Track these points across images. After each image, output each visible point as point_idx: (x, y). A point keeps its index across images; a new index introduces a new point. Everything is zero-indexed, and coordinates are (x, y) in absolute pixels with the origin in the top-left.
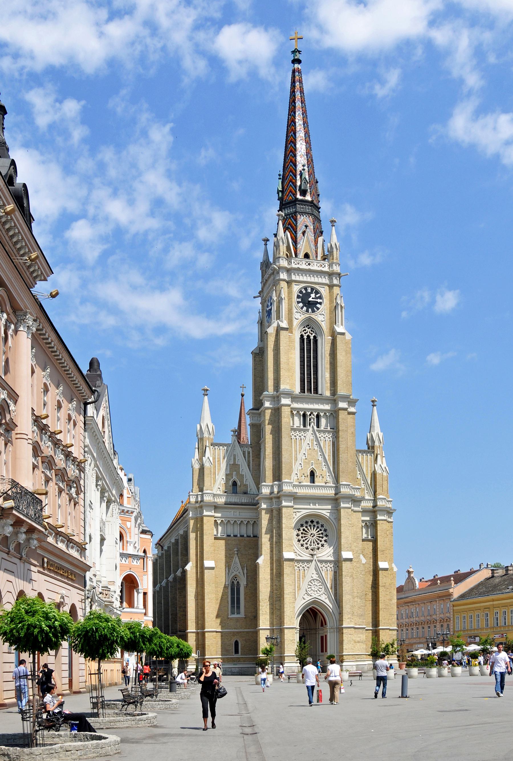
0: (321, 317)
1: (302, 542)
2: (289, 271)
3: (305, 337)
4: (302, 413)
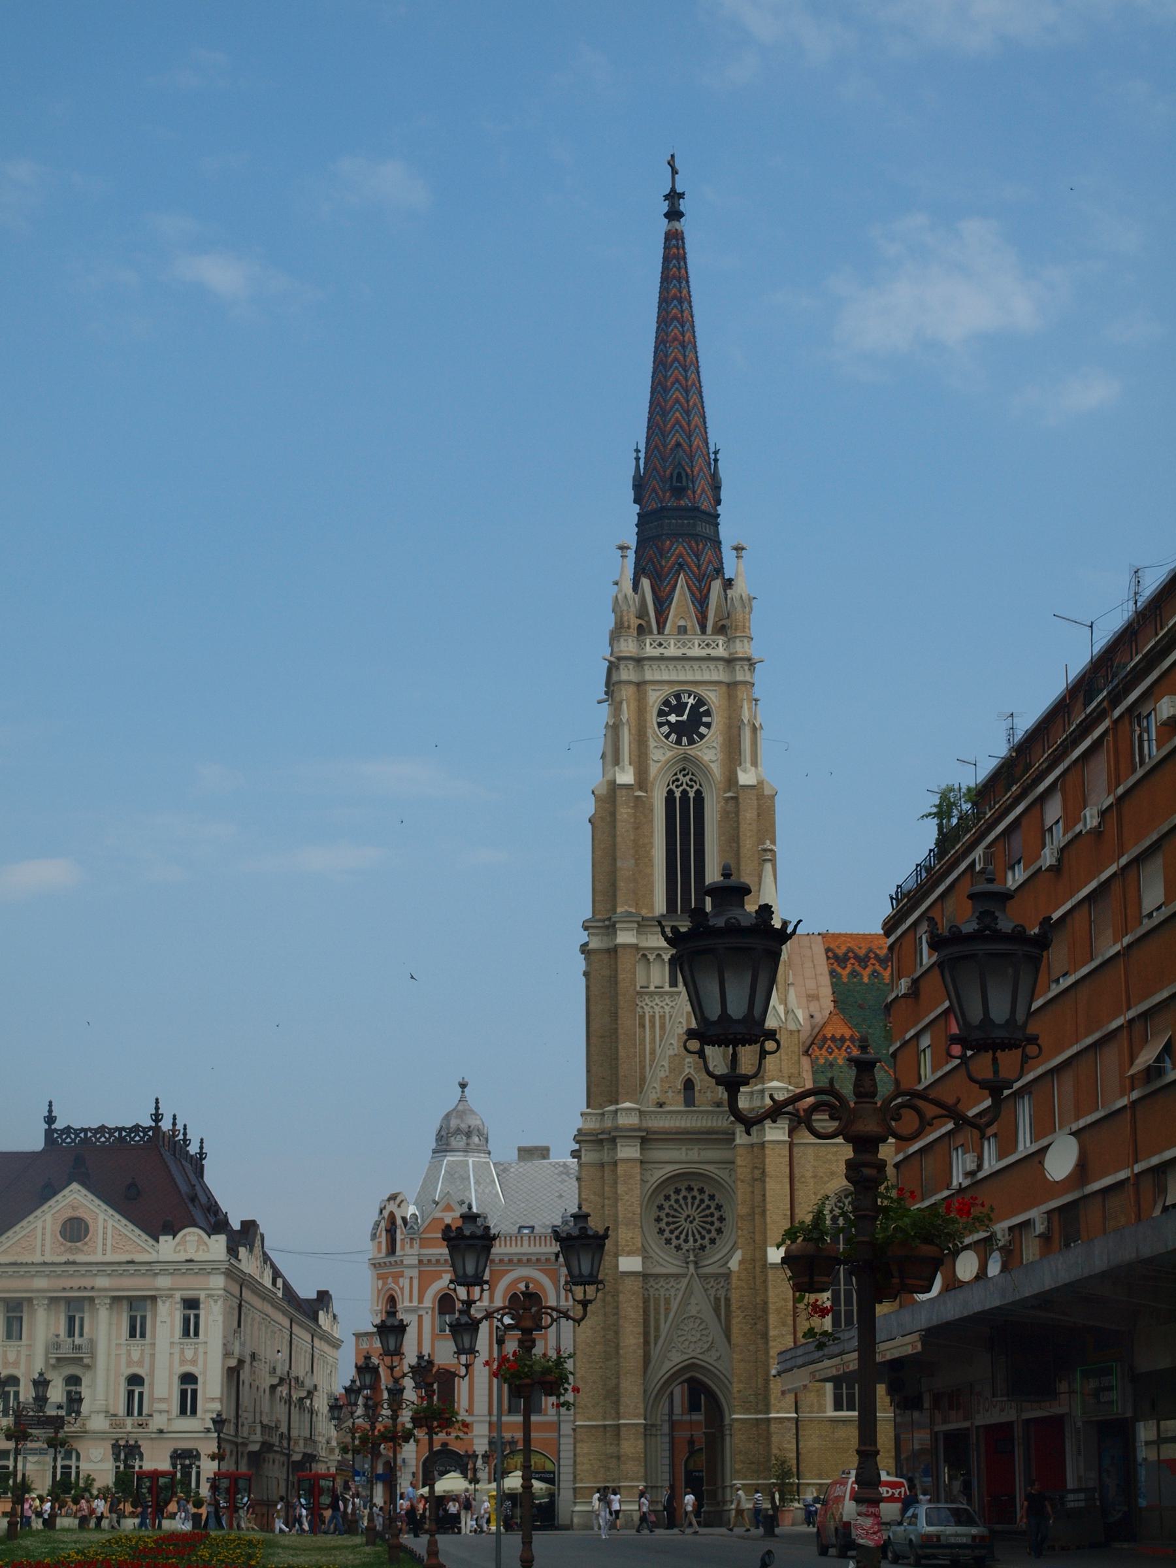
0: (709, 751)
1: (667, 1234)
2: (639, 661)
3: (678, 795)
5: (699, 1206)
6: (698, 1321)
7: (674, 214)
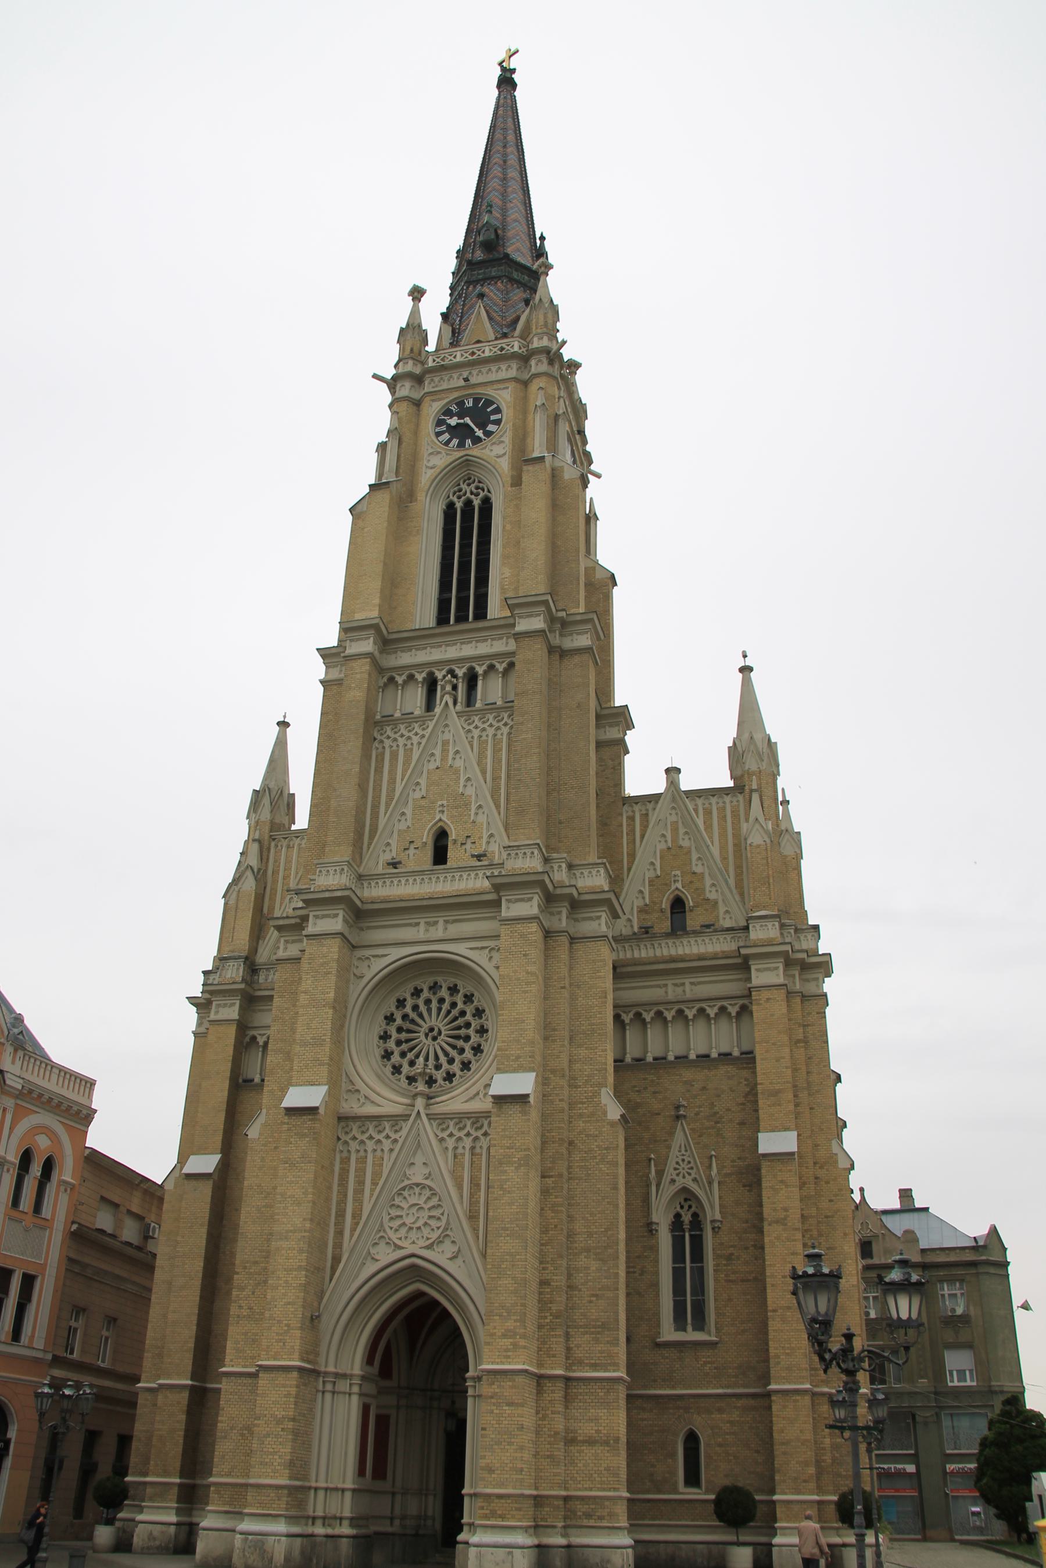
1: (396, 1058)
3: (459, 505)
4: (420, 677)
5: (449, 1012)
6: (428, 1193)
7: (507, 82)
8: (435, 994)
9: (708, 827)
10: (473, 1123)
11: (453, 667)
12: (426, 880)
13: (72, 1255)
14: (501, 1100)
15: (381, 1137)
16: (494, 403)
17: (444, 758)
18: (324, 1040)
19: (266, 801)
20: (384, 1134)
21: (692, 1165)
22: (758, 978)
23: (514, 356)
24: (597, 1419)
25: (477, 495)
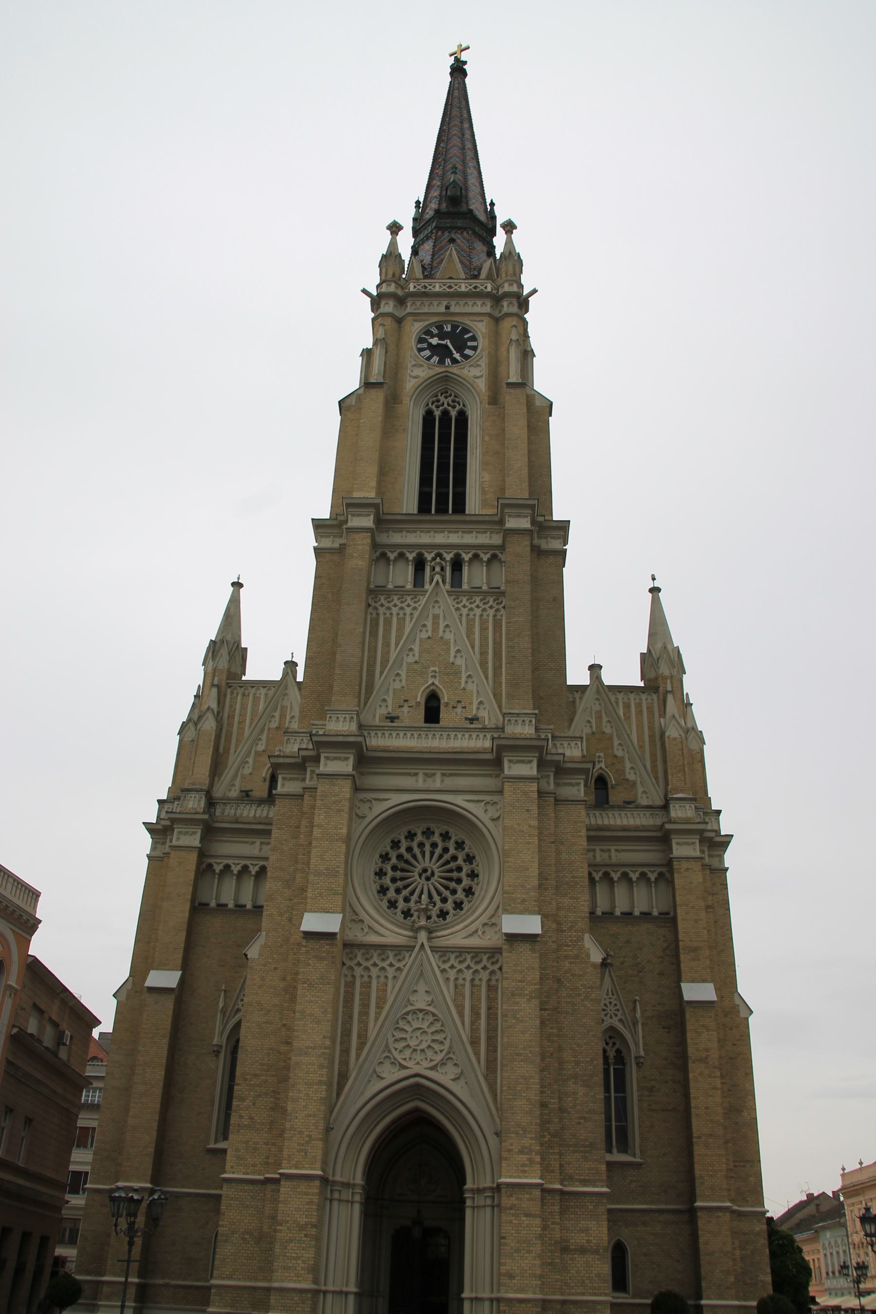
1: (391, 894)
3: (437, 413)
4: (411, 556)
5: (441, 856)
6: (431, 1019)
7: (458, 70)
8: (428, 838)
9: (628, 718)
10: (473, 958)
11: (442, 551)
12: (423, 736)
13: (11, 1059)
14: (513, 938)
15: (385, 965)
16: (469, 332)
17: (435, 629)
18: (338, 872)
19: (224, 651)
20: (388, 962)
21: (618, 1007)
22: (678, 850)
23: (488, 295)
24: (586, 1230)
25: (454, 407)
